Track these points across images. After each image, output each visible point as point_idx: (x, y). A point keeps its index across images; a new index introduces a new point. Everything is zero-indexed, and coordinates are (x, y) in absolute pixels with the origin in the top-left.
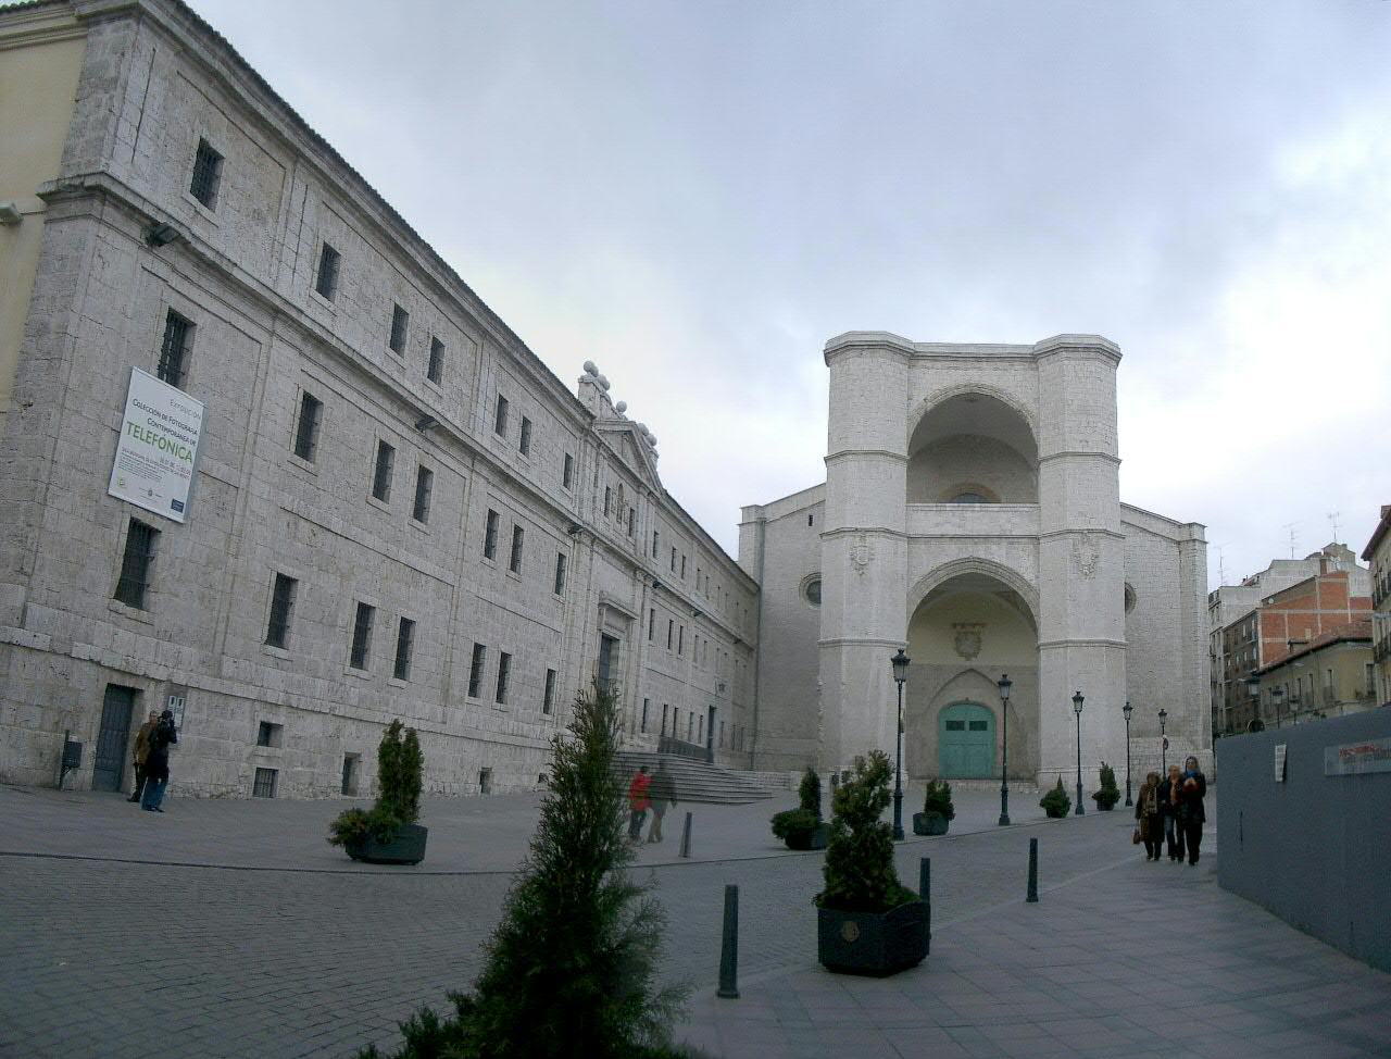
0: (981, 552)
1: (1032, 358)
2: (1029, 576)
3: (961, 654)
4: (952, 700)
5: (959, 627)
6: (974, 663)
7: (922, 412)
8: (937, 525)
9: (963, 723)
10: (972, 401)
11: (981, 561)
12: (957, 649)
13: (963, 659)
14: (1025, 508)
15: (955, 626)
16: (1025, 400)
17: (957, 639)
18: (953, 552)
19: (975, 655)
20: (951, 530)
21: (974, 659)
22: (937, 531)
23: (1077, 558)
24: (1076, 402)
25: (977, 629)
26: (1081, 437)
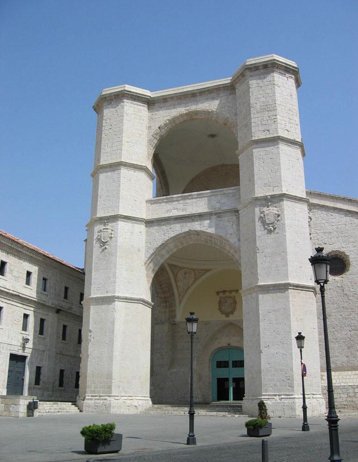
0: (197, 226)
1: (231, 88)
2: (233, 240)
3: (223, 313)
4: (220, 346)
5: (221, 295)
6: (232, 318)
7: (158, 137)
8: (168, 211)
9: (228, 362)
10: (213, 136)
11: (198, 233)
12: (220, 309)
13: (224, 316)
14: (229, 190)
15: (218, 293)
16: (228, 115)
17: (220, 302)
18: (177, 229)
19: (232, 313)
20: (175, 213)
21: (230, 315)
22: (167, 215)
23: (262, 220)
24: (259, 104)
25: (234, 294)
26: (264, 128)
